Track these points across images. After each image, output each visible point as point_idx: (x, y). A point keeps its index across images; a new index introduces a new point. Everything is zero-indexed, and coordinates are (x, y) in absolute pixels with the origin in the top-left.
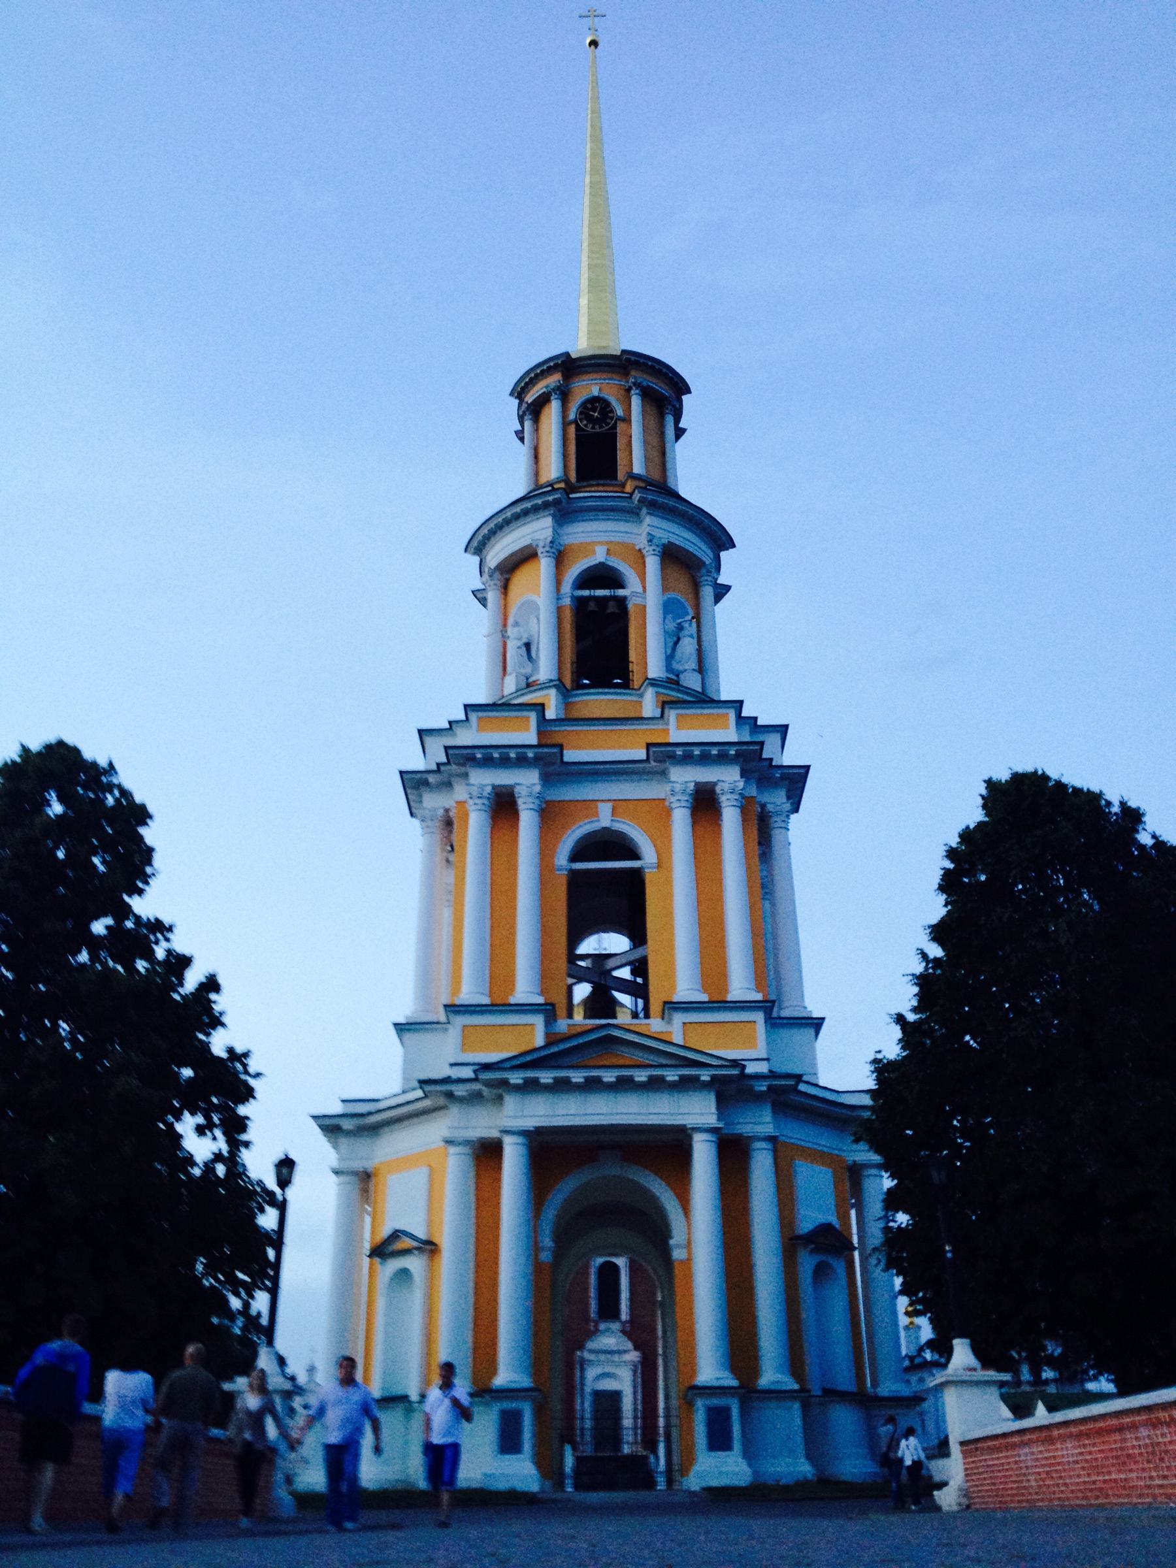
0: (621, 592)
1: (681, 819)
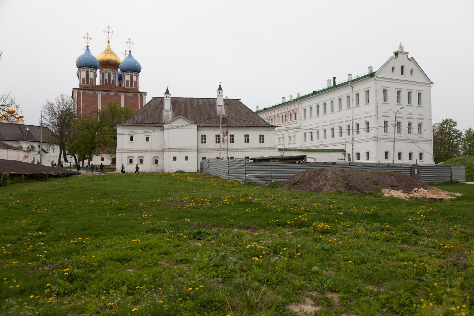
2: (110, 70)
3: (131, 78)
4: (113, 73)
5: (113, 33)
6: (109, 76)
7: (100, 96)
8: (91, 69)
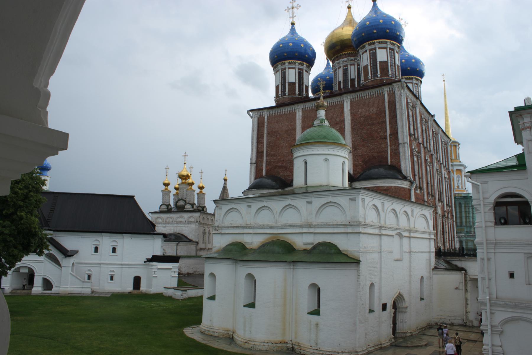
2: (345, 59)
4: (354, 65)
6: (346, 73)
7: (299, 115)
8: (290, 63)
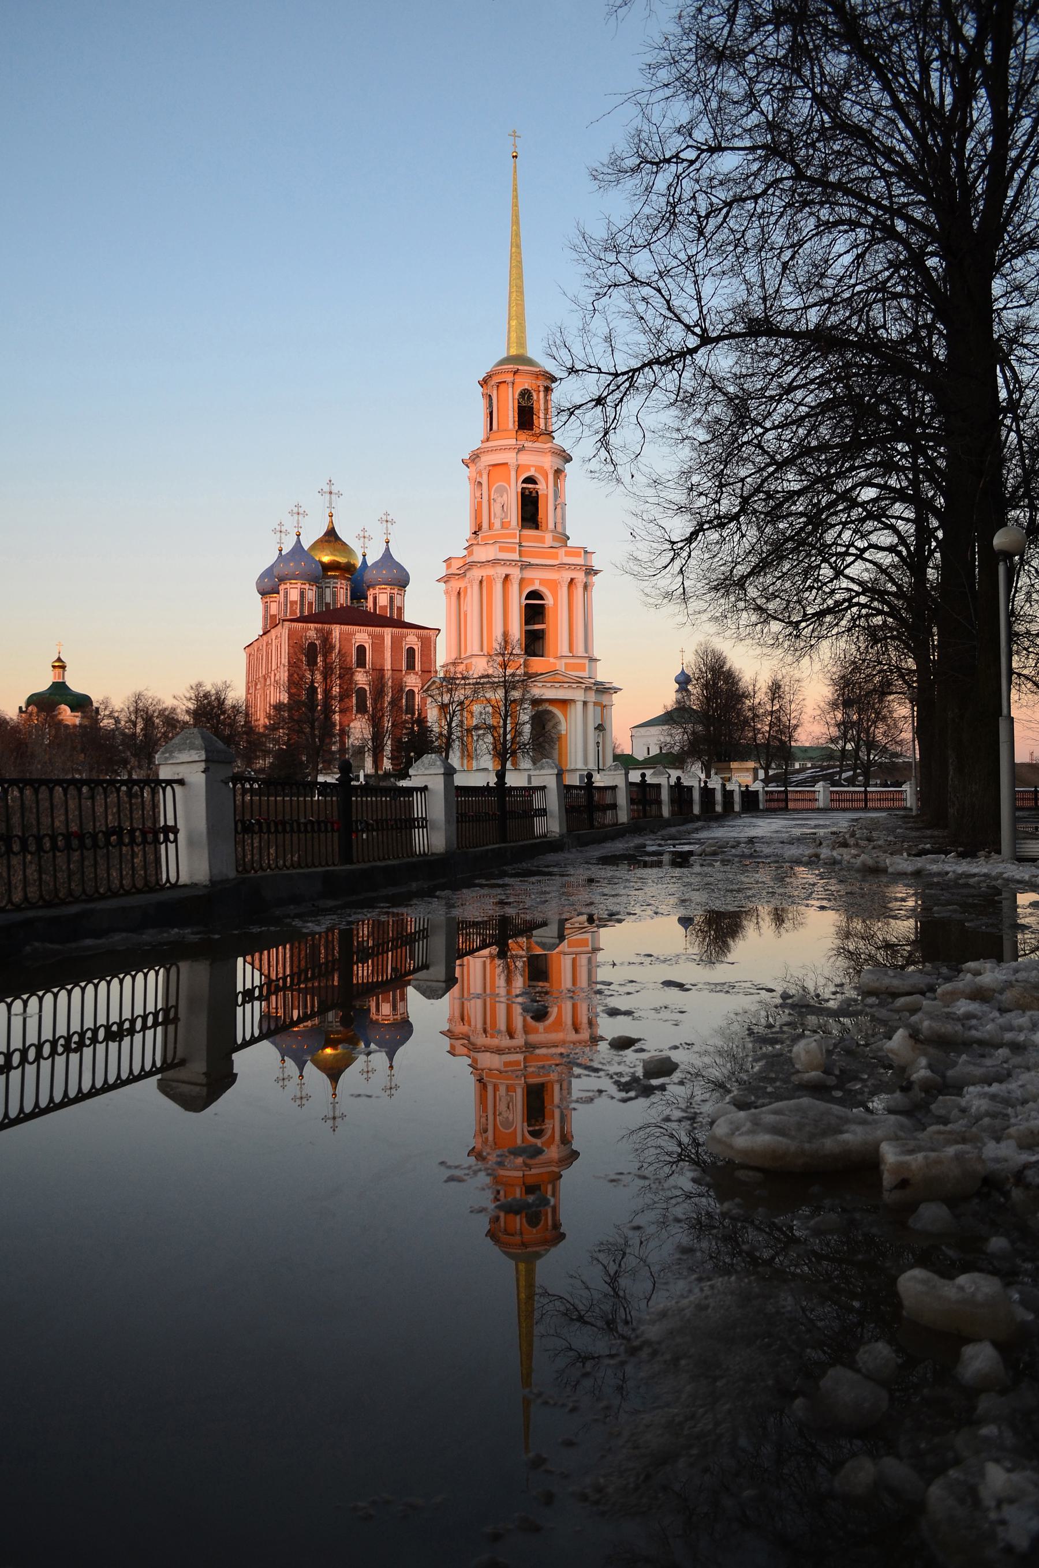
0: (537, 486)
1: (564, 591)
3: (391, 600)
5: (339, 495)
